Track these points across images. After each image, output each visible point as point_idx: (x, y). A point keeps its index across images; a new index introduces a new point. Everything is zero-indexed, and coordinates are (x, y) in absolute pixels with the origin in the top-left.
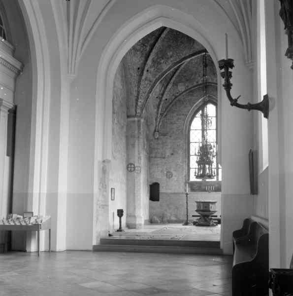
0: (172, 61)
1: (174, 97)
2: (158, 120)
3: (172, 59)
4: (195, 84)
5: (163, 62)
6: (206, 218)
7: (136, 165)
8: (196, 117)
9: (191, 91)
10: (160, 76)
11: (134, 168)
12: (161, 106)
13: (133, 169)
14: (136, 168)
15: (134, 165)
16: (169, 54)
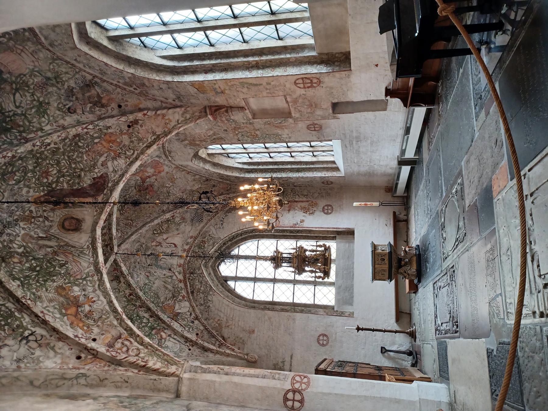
0: (94, 291)
1: (196, 322)
2: (228, 351)
3: (90, 289)
4: (182, 285)
5: (90, 306)
6: (403, 263)
7: (291, 388)
8: (234, 290)
9: (192, 293)
10: (115, 317)
11: (294, 391)
12: (206, 344)
13: (298, 397)
14: (297, 386)
15: (288, 391)
16: (76, 294)
